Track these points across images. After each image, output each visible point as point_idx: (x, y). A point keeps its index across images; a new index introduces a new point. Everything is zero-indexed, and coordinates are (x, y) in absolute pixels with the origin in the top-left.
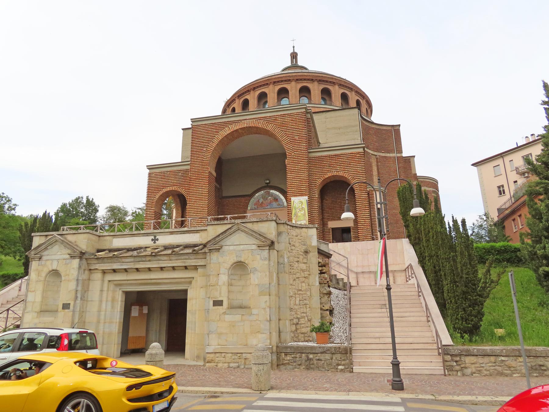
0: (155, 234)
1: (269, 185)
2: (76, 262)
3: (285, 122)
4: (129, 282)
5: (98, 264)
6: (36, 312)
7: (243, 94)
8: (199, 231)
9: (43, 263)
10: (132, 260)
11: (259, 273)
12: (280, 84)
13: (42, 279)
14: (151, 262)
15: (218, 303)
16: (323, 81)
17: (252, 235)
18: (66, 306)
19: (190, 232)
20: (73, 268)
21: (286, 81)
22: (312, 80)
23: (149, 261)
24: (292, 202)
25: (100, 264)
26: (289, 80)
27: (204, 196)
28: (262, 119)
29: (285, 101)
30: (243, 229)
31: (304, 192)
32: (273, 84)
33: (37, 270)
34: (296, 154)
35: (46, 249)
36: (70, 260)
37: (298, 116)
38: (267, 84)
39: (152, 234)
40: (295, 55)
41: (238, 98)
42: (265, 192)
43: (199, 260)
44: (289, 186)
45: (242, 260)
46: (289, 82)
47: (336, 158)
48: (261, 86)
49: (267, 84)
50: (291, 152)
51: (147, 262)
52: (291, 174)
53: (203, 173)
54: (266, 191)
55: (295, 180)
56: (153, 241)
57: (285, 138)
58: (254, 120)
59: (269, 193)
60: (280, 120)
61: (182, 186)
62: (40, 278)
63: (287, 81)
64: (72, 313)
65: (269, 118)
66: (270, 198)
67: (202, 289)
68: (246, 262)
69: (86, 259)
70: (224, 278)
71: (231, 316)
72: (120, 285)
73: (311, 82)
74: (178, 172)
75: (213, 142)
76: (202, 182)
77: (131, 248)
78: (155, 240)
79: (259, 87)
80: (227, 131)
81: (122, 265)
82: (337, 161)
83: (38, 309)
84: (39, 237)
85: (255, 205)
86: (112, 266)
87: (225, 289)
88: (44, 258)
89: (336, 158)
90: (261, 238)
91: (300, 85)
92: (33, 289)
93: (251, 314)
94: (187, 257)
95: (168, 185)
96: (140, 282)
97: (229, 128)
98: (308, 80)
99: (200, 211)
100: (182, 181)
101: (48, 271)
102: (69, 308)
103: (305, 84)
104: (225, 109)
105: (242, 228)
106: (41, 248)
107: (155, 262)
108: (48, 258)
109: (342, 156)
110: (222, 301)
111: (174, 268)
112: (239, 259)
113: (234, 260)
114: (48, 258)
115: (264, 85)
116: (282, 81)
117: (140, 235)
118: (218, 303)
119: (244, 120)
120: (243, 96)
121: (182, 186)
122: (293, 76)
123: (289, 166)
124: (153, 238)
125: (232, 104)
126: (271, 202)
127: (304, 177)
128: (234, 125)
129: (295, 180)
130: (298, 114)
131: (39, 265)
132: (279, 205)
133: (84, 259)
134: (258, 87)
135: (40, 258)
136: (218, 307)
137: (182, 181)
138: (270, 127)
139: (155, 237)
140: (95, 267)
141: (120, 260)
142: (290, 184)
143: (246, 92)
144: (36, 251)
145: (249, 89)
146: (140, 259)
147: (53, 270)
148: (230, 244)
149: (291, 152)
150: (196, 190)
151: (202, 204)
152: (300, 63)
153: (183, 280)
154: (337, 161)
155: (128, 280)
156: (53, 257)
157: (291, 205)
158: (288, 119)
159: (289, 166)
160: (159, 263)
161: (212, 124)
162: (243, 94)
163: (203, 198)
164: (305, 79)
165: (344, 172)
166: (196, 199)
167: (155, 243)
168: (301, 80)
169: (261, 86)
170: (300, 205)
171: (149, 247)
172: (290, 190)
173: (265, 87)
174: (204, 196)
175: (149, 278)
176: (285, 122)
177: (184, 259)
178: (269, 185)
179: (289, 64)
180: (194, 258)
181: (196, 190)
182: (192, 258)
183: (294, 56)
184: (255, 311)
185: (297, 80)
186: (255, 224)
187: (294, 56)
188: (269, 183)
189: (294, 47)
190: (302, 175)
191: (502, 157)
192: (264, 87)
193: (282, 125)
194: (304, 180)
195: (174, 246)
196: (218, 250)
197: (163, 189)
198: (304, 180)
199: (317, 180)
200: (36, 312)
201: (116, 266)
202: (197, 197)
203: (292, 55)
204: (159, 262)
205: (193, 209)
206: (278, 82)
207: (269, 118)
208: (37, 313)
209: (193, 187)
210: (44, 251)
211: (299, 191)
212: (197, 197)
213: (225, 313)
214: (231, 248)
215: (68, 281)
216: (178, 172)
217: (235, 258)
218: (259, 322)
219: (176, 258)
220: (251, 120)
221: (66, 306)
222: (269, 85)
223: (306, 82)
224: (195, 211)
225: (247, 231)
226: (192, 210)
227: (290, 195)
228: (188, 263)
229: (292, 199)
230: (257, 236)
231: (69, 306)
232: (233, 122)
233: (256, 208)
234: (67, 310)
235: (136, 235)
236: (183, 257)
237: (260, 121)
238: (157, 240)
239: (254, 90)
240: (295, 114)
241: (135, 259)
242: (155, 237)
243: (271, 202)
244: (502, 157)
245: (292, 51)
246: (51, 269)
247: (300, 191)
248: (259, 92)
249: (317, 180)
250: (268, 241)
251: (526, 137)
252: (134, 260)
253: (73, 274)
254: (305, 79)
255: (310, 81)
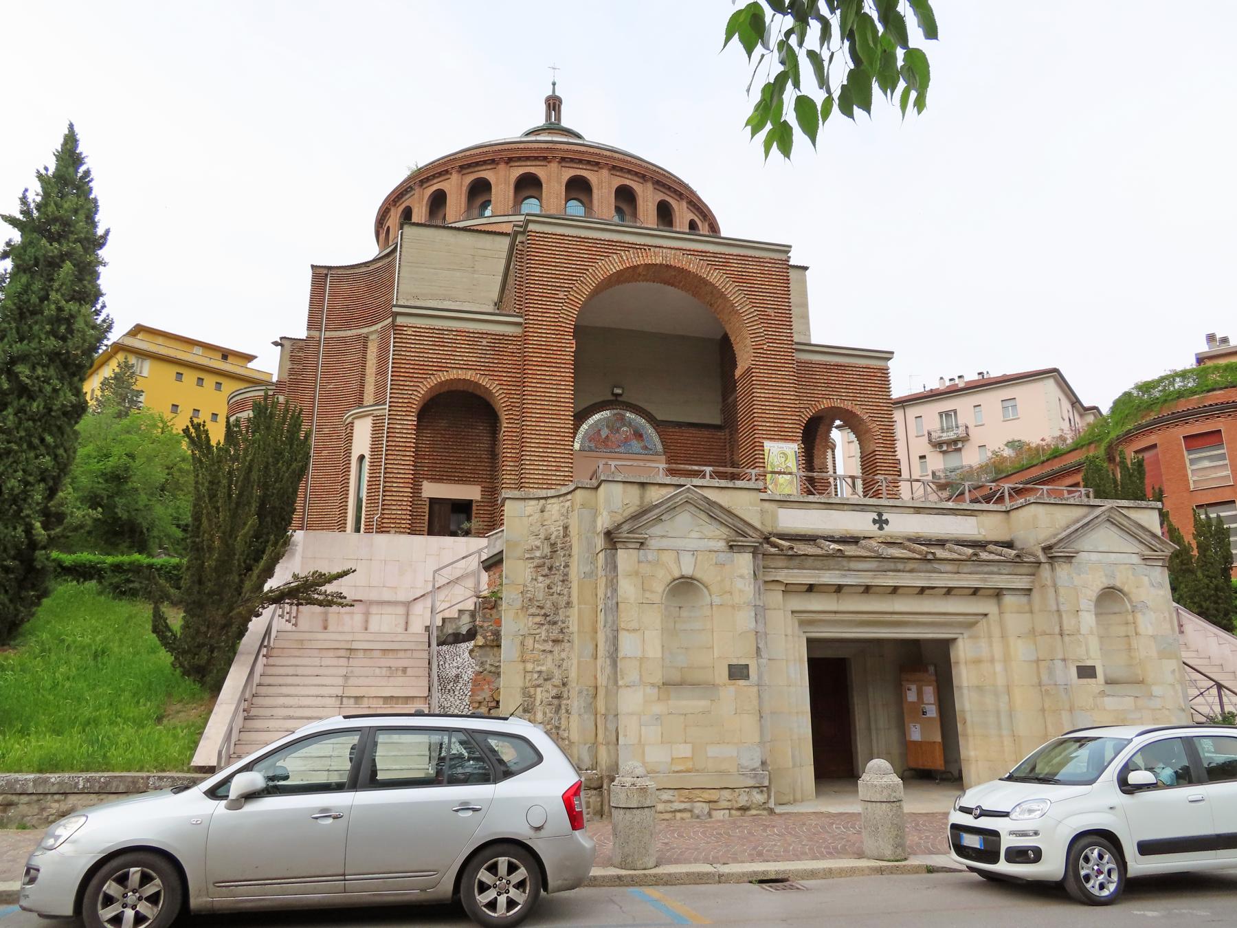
0: (881, 509)
1: (620, 399)
2: (744, 562)
3: (747, 274)
4: (838, 617)
5: (786, 571)
6: (653, 685)
7: (477, 164)
8: (976, 513)
9: (651, 556)
10: (873, 565)
11: (1152, 613)
12: (575, 166)
13: (656, 598)
14: (915, 574)
15: (1086, 672)
16: (664, 185)
17: (1134, 536)
18: (738, 672)
19: (957, 512)
20: (742, 577)
21: (589, 162)
22: (644, 177)
23: (911, 571)
24: (766, 453)
25: (791, 571)
26: (597, 164)
27: (563, 409)
28: (696, 253)
29: (531, 206)
30: (1120, 520)
31: (790, 434)
32: (559, 162)
33: (637, 573)
34: (772, 349)
35: (659, 519)
36: (730, 555)
37: (773, 265)
38: (545, 158)
39: (874, 509)
40: (557, 103)
41: (459, 172)
42: (615, 415)
43: (1015, 577)
44: (760, 415)
45: (1118, 584)
46: (596, 169)
47: (840, 372)
48: (528, 158)
49: (545, 158)
50: (761, 342)
51: (904, 574)
52: (762, 391)
53: (559, 353)
54: (615, 411)
55: (771, 404)
56: (884, 525)
57: (747, 308)
58: (678, 252)
59: (622, 418)
60: (735, 266)
61: (491, 373)
62: (647, 595)
63: (592, 165)
64: (755, 689)
65: (712, 255)
66: (625, 429)
67: (1019, 642)
68: (1126, 589)
69: (764, 555)
70: (1088, 619)
71: (1115, 699)
72: (811, 623)
73: (641, 181)
74: (480, 336)
75: (581, 281)
76: (558, 374)
77: (833, 537)
78: (881, 522)
79: (524, 161)
80: (615, 264)
81: (845, 576)
82: (840, 379)
83: (657, 678)
84: (620, 486)
85: (590, 441)
86: (819, 577)
87: (1094, 643)
88: (653, 543)
89: (840, 372)
90: (1153, 542)
91: (568, 173)
92: (634, 625)
93: (1152, 695)
94: (995, 569)
95: (453, 366)
96: (865, 617)
97: (622, 257)
98: (636, 174)
99: (554, 442)
100: (491, 361)
101: (669, 578)
102: (747, 677)
103: (628, 182)
104: (410, 187)
105: (1116, 517)
106: (649, 515)
107: (922, 574)
108: (665, 543)
109: (850, 369)
110: (1094, 667)
111: (949, 591)
112: (1111, 583)
113: (1102, 582)
114: (665, 543)
115: (536, 158)
116: (580, 161)
117: (846, 507)
118: (1086, 672)
119: (656, 247)
120: (476, 169)
121: (491, 373)
122: (606, 157)
123: (757, 371)
124: (877, 518)
125: (435, 181)
126: (626, 440)
127: (788, 401)
128: (634, 253)
129: (771, 404)
130: (773, 261)
131: (639, 562)
132: (646, 448)
133: (761, 556)
134: (519, 159)
135: (642, 544)
136: (1089, 680)
137: (491, 361)
138: (715, 277)
139: (880, 515)
140: (775, 576)
141: (845, 563)
142: (760, 411)
143: (485, 162)
144: (636, 522)
145: (497, 158)
146: (892, 566)
147: (683, 577)
148: (1091, 548)
149: (761, 342)
150: (542, 390)
151: (558, 425)
152: (565, 123)
153: (961, 619)
154: (840, 379)
155: (835, 612)
156: (679, 543)
157: (764, 459)
158: (753, 268)
159: (757, 371)
160: (929, 579)
161: (580, 237)
162: (477, 164)
163: (562, 413)
164: (629, 171)
165: (854, 402)
166: (542, 411)
167: (881, 528)
168: (621, 169)
169: (528, 158)
170: (783, 460)
171: (870, 538)
172: (760, 424)
173: (538, 163)
174: (563, 409)
175: (890, 609)
176: (747, 274)
177: (986, 573)
178: (620, 399)
179: (540, 121)
180: (1007, 572)
181: (542, 390)
182: (1004, 572)
183: (554, 104)
184: (1157, 690)
185: (614, 168)
186: (1132, 510)
187: (554, 104)
188: (620, 395)
189: (554, 84)
190: (785, 397)
191: (904, 407)
192: (534, 163)
193: (739, 279)
194: (789, 407)
195: (930, 540)
196: (1069, 559)
197: (440, 373)
198: (789, 407)
199: (802, 410)
200: (653, 685)
201: (830, 577)
202: (546, 407)
203: (551, 102)
204: (932, 575)
205: (538, 437)
206: (572, 160)
207: (712, 255)
208: (656, 690)
209: (535, 381)
210: (652, 526)
211: (780, 429)
212: (546, 407)
213: (1103, 694)
214: (1094, 557)
215: (733, 607)
216: (480, 336)
217: (1104, 579)
218: (1167, 712)
219: (973, 569)
220: (673, 252)
221: (738, 672)
222: (549, 162)
223: (630, 177)
224: (542, 441)
225: (1127, 525)
226: (533, 436)
227: (760, 436)
228: (991, 582)
229: (765, 444)
230: (1146, 537)
231: (745, 671)
232: (630, 246)
233: (593, 448)
234: (742, 682)
235: (834, 507)
236: (986, 569)
237: (693, 258)
238: (887, 522)
239: (507, 163)
240: (769, 260)
241: (882, 564)
242: (880, 515)
243: (626, 440)
244: (904, 407)
245: (550, 93)
246: (677, 575)
247: (783, 429)
248: (521, 173)
249: (802, 410)
250: (1166, 550)
251: (941, 378)
252: (878, 567)
253: (741, 591)
254: (629, 171)
255: (639, 177)
